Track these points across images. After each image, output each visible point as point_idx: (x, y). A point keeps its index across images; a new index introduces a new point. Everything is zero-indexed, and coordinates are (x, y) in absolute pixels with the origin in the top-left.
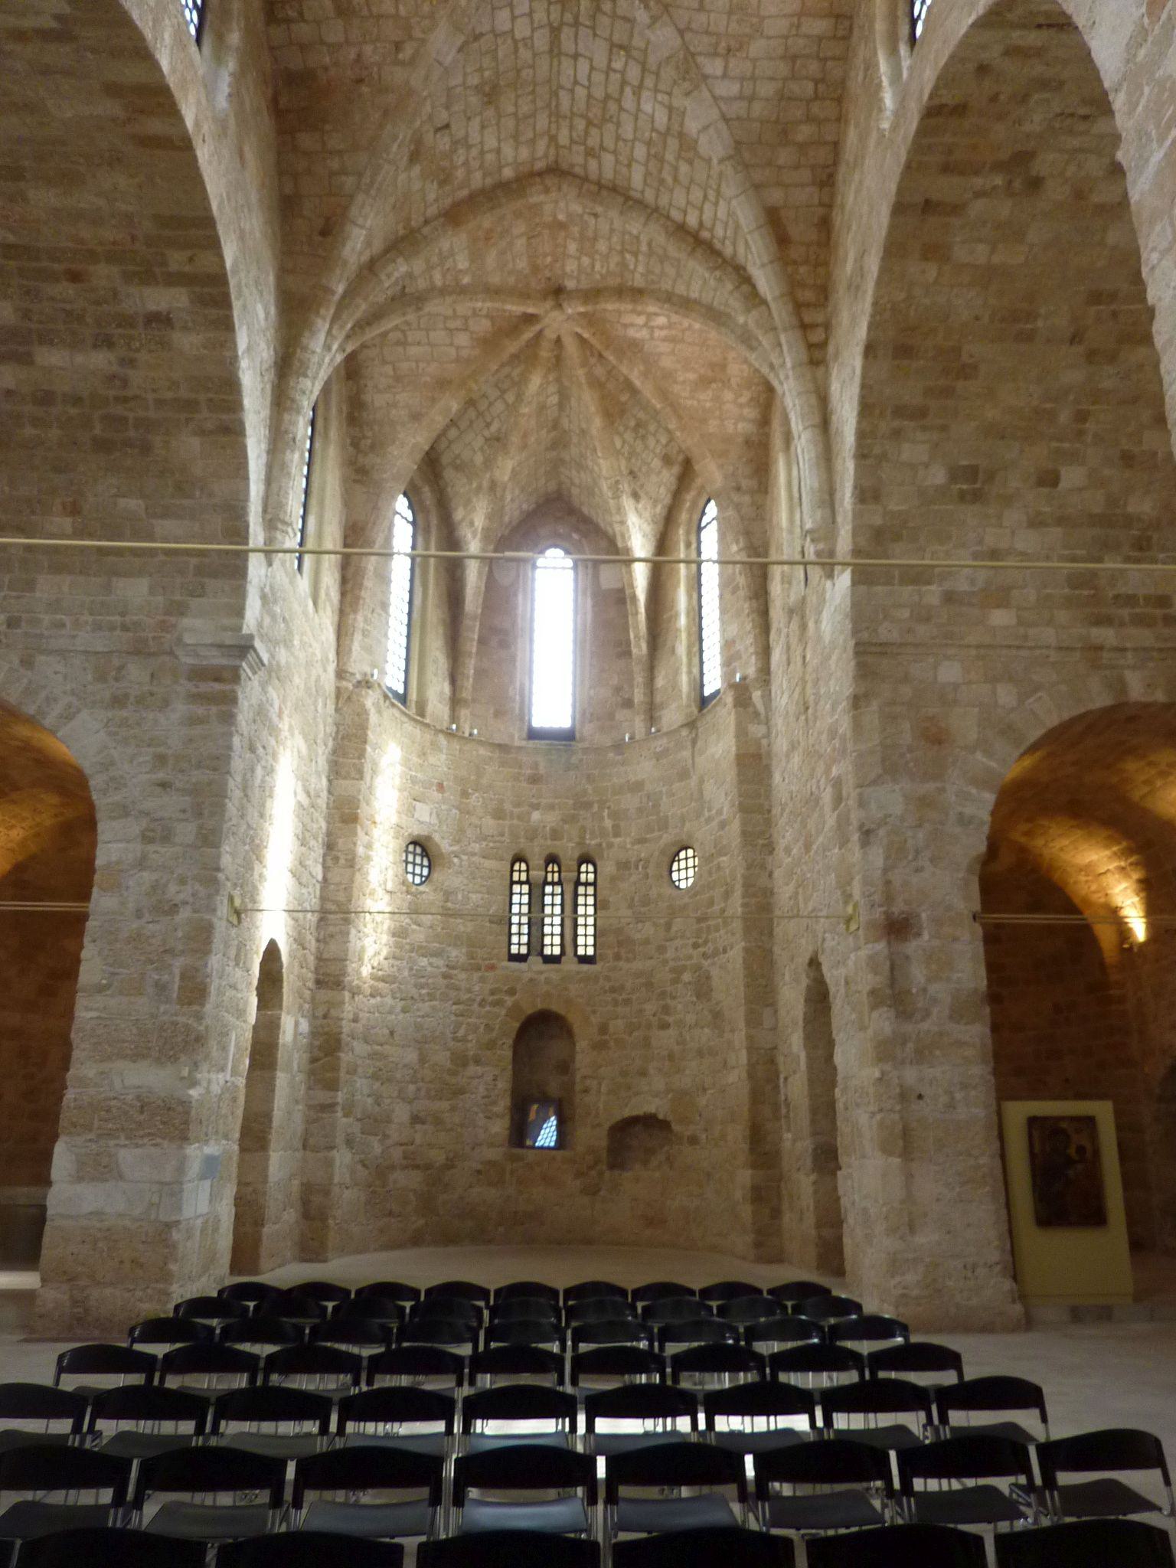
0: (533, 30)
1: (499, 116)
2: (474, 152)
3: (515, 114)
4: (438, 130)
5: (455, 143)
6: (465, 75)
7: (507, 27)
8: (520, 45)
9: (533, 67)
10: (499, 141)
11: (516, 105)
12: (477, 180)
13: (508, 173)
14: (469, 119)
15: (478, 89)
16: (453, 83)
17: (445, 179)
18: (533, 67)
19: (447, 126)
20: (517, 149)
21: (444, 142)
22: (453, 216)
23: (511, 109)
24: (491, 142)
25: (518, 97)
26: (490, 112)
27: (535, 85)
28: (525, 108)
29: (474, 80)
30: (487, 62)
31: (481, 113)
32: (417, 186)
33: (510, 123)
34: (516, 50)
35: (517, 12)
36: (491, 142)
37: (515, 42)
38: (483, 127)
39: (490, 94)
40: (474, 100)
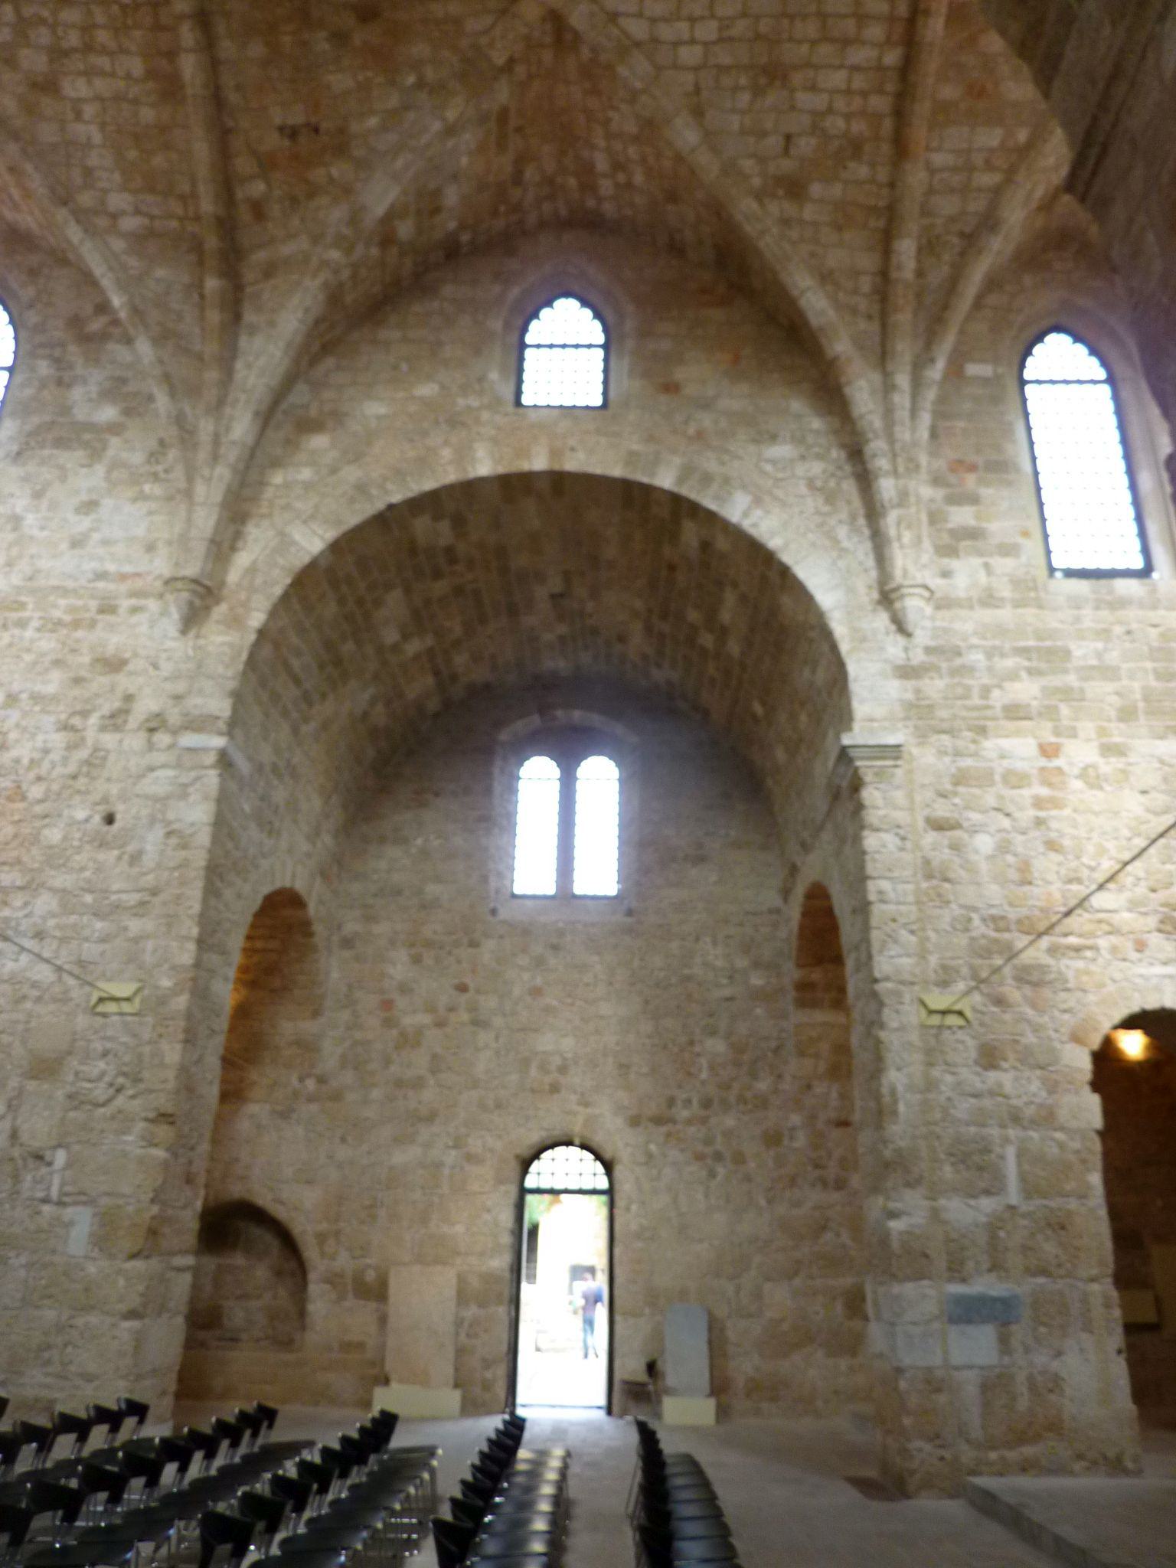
0: (713, 16)
1: (809, 65)
2: (840, 104)
3: (814, 43)
4: (786, 151)
5: (815, 129)
6: (733, 111)
7: (698, 50)
8: (726, 34)
9: (758, 18)
10: (841, 67)
11: (800, 42)
12: (880, 103)
13: (892, 57)
14: (793, 108)
15: (758, 92)
16: (736, 126)
17: (855, 148)
18: (758, 18)
19: (788, 138)
20: (863, 43)
21: (806, 145)
22: (901, 149)
23: (804, 49)
24: (838, 79)
25: (791, 39)
26: (797, 78)
27: (784, 15)
28: (811, 29)
29: (745, 98)
30: (727, 81)
31: (792, 91)
32: (837, 190)
33: (825, 50)
34: (731, 39)
35: (686, 36)
36: (838, 79)
37: (721, 40)
38: (813, 88)
39: (773, 74)
40: (771, 98)
